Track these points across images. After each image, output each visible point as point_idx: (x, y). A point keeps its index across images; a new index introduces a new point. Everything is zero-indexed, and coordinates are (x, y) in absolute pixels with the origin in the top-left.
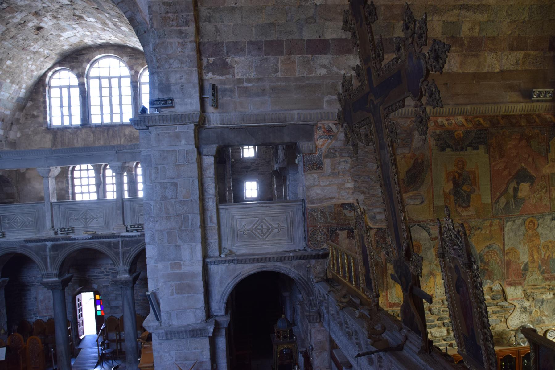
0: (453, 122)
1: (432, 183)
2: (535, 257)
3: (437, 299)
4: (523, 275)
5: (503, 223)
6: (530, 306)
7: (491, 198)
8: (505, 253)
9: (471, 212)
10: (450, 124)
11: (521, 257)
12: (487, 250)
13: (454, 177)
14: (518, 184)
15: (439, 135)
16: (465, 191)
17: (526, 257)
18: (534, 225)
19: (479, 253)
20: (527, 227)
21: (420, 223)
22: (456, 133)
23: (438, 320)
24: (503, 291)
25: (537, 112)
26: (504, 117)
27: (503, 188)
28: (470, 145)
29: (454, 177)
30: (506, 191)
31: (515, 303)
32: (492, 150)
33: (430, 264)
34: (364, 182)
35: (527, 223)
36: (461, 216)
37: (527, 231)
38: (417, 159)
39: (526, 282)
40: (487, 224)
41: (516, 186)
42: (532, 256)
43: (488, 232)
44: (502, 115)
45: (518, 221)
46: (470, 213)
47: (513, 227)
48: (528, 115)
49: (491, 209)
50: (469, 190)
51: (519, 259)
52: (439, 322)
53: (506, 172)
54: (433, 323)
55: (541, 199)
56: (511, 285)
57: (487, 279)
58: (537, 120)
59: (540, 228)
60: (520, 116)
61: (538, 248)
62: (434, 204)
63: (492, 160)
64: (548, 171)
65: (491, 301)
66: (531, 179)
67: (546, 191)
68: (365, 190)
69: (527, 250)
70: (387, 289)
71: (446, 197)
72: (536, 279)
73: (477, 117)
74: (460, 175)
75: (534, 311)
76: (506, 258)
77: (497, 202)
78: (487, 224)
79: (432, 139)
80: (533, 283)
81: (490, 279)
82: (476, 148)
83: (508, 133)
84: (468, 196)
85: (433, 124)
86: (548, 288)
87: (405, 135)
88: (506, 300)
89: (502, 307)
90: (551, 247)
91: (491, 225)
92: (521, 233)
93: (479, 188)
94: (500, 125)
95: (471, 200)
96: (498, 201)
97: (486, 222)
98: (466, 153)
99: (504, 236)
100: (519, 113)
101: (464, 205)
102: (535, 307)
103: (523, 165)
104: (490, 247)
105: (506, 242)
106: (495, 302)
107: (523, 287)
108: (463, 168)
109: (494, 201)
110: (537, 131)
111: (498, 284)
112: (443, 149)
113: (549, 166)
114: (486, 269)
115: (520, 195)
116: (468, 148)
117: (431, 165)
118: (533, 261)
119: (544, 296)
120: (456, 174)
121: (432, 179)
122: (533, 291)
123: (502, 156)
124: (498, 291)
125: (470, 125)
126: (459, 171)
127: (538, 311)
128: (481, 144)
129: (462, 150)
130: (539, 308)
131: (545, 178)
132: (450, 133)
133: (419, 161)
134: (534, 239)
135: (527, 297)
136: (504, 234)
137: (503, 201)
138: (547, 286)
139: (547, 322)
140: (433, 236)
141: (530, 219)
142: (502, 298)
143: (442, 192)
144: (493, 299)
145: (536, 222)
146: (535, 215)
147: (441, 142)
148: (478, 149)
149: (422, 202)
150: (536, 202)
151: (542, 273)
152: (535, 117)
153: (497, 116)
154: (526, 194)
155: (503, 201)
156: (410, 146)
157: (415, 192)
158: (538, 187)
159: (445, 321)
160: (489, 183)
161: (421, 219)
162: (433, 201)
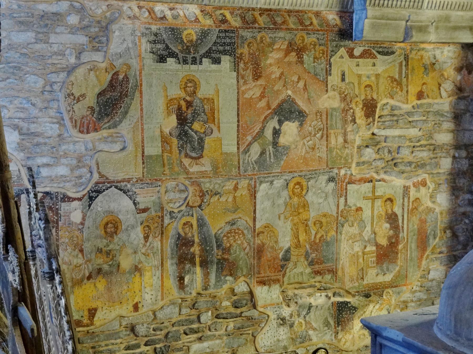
0: (181, 13)
1: (142, 117)
2: (301, 239)
3: (144, 310)
4: (282, 267)
5: (255, 187)
6: (291, 316)
7: (238, 144)
8: (256, 233)
9: (205, 165)
10: (175, 17)
11: (280, 239)
13: (180, 108)
14: (280, 123)
15: (156, 35)
17: (288, 238)
18: (302, 189)
20: (291, 193)
21: (119, 184)
22: (185, 32)
23: (146, 345)
24: (251, 293)
25: (315, 9)
26: (263, 11)
27: (257, 129)
28: (208, 54)
29: (180, 108)
31: (269, 311)
32: (242, 65)
33: (135, 252)
34: (23, 109)
35: (291, 185)
36: (187, 173)
37: (290, 198)
38: (116, 74)
39: (286, 279)
40: (230, 186)
41: (277, 127)
42: (297, 237)
43: (230, 199)
44: (261, 9)
45: (278, 183)
46: (203, 169)
48: (302, 11)
49: (236, 163)
50: (202, 131)
51: (276, 242)
52: (148, 348)
53: (262, 104)
55: (313, 149)
56: (262, 283)
57: (226, 276)
58: (315, 21)
59: (310, 194)
60: (289, 12)
61: (307, 225)
62: (143, 152)
63: (241, 81)
64: (326, 105)
65: (232, 310)
66: (300, 116)
67: (322, 137)
68: (21, 124)
69: (289, 228)
71: (165, 140)
72: (302, 273)
73: (220, 8)
74: (189, 104)
75: (297, 322)
76: (258, 241)
77: (246, 151)
79: (144, 40)
80: (296, 280)
81: (231, 275)
82: (217, 61)
83: (268, 40)
84: (201, 141)
85: (147, 14)
86: (319, 287)
87: (97, 29)
88: (255, 307)
89: (250, 319)
90: (324, 224)
91: (236, 188)
92: (281, 201)
93: (219, 127)
94: (256, 25)
95: (206, 146)
96: (248, 150)
97: (228, 183)
98: (201, 67)
99: (255, 206)
100: (288, 8)
101: (194, 155)
102: (299, 315)
103: (289, 92)
104: (232, 223)
105: (258, 215)
106: (238, 311)
107: (281, 286)
108: (195, 92)
109: (241, 150)
110: (312, 39)
111: (243, 283)
112: (162, 59)
113: (329, 97)
114: (224, 259)
115: (282, 140)
116: (204, 60)
117: (141, 85)
118: (298, 245)
119: (312, 300)
120: (183, 103)
121: (142, 110)
122: (296, 292)
123: (257, 76)
124: (244, 293)
125: (208, 22)
126: (188, 98)
127: (303, 322)
128: (226, 54)
129: (194, 62)
130: (305, 317)
131: (321, 116)
132: (175, 32)
133: (121, 77)
134: (301, 211)
135: (288, 301)
136: (255, 203)
137: (256, 149)
138: (317, 284)
139: (315, 339)
140: (142, 206)
141: (295, 180)
142: (250, 304)
143: (158, 133)
144: (236, 307)
145: (304, 184)
146: (303, 173)
147: (159, 46)
148: (219, 63)
149: (123, 149)
150: (307, 152)
151: (311, 263)
152: (310, 15)
153: (253, 9)
154: (291, 139)
155: (256, 149)
156: (105, 49)
157: (112, 131)
158: (310, 129)
160: (236, 119)
161: (120, 176)
162: (143, 146)
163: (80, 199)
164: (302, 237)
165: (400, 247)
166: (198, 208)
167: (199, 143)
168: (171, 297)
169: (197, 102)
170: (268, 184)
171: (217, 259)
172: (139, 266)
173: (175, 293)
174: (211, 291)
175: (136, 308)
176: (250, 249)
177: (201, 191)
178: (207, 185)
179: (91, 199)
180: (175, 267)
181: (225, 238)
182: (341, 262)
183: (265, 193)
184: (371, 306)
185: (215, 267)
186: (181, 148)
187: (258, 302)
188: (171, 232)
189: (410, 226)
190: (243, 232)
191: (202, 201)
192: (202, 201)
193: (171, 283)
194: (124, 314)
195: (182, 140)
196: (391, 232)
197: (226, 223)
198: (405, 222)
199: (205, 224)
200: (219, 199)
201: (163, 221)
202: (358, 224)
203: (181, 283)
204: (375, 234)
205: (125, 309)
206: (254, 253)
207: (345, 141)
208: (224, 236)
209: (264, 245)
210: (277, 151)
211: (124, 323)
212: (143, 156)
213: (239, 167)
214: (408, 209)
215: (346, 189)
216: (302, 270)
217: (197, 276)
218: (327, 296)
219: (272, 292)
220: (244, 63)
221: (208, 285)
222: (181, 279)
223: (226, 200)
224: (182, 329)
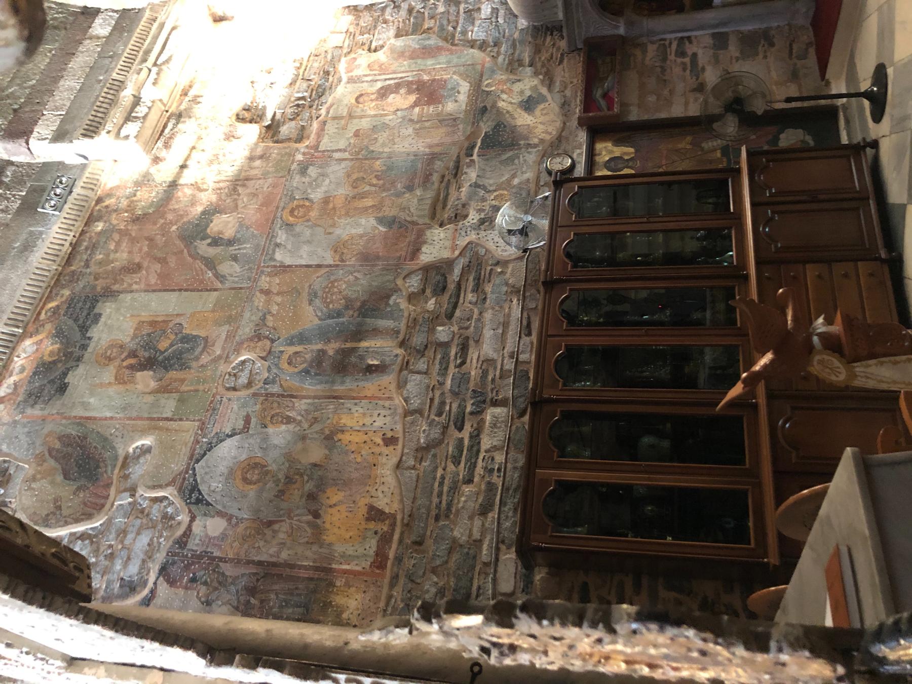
2: (370, 204)
3: (399, 427)
5: (275, 266)
6: (480, 211)
7: (210, 290)
12: (317, 302)
16: (171, 345)
17: (363, 221)
19: (320, 319)
23: (460, 429)
27: (199, 264)
28: (84, 329)
29: (131, 367)
30: (210, 263)
31: (462, 242)
40: (260, 300)
41: (209, 241)
42: (366, 209)
43: (279, 299)
45: (281, 237)
46: (224, 336)
47: (289, 247)
49: (233, 292)
50: (173, 337)
53: (172, 262)
54: (466, 442)
56: (416, 252)
57: (387, 304)
62: (167, 419)
65: (446, 297)
70: (329, 571)
71: (164, 389)
75: (493, 203)
78: (260, 300)
81: (388, 297)
84: (186, 339)
91: (267, 292)
92: (308, 232)
101: (199, 349)
102: (484, 200)
106: (452, 286)
109: (219, 285)
112: (63, 388)
114: (361, 307)
115: (229, 233)
118: (378, 207)
129: (84, 347)
130: (489, 191)
136: (296, 266)
140: (240, 424)
143: (150, 399)
159: (468, 409)
161: (185, 452)
163: (193, 519)
164: (369, 202)
165: (426, 78)
166: (274, 345)
167: (187, 342)
168: (393, 387)
169: (132, 346)
170: (277, 250)
171: (358, 317)
172: (327, 432)
173: (388, 380)
174: (403, 326)
175: (390, 441)
176: (359, 272)
177: (251, 339)
178: (247, 330)
179: (200, 501)
180: (348, 380)
181: (331, 306)
182: (422, 149)
183: (288, 254)
184: (501, 104)
185: (368, 320)
186: (184, 366)
187: (443, 259)
188: (295, 383)
189: (403, 69)
190: (332, 282)
191: (267, 338)
192: (267, 338)
193: (371, 386)
194: (395, 460)
195: (174, 364)
196: (402, 91)
197: (310, 304)
198: (394, 76)
199: (300, 334)
200: (273, 315)
201: (273, 395)
202: (375, 133)
203: (376, 371)
204: (398, 110)
205: (389, 458)
206: (367, 266)
207: (261, 157)
208: (327, 307)
209: (361, 253)
210: (239, 240)
211: (411, 462)
212: (171, 420)
213: (241, 288)
214: (380, 75)
215: (324, 151)
216: (416, 201)
217: (373, 345)
218: (468, 166)
219: (435, 238)
220: (114, 284)
221: (393, 329)
222: (370, 369)
223: (278, 305)
224: (452, 370)
